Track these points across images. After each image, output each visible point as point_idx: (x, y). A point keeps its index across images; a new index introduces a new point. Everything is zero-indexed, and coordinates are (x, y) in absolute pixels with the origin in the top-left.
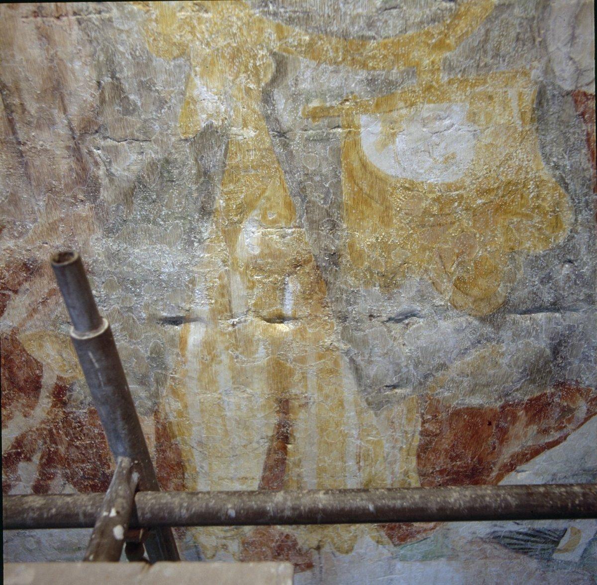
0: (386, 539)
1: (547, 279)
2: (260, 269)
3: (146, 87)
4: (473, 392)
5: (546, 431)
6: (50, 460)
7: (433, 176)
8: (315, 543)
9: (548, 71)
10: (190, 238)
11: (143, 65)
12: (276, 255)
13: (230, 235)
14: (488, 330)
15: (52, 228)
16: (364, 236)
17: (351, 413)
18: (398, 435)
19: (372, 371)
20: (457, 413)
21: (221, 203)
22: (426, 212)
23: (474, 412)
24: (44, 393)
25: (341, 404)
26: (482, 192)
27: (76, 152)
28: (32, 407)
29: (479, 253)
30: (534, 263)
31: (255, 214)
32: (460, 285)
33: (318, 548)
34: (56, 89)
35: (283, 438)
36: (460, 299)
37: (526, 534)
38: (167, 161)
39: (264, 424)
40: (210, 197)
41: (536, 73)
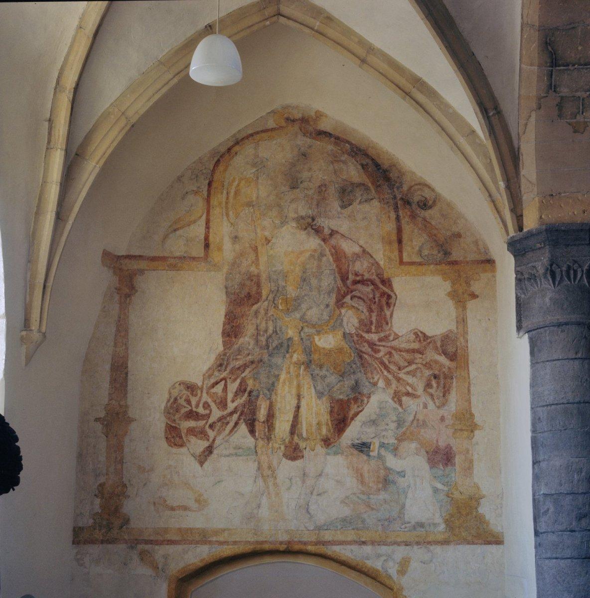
0: (323, 445)
1: (351, 367)
2: (296, 364)
3: (281, 331)
4: (340, 394)
5: (358, 407)
6: (241, 414)
7: (327, 346)
8: (304, 447)
9: (345, 330)
10: (284, 357)
11: (281, 328)
12: (299, 361)
13: (291, 357)
14: (341, 378)
15: (259, 354)
16: (315, 357)
17: (314, 400)
18: (324, 407)
19: (318, 388)
20: (338, 401)
21: (290, 350)
22: (327, 353)
23: (341, 400)
24: (247, 393)
25: (312, 397)
26: (337, 349)
27: (267, 341)
28: (242, 396)
29: (337, 361)
30: (348, 364)
31: (296, 353)
32: (334, 368)
33: (305, 448)
34: (266, 331)
35: (298, 407)
36: (335, 371)
37: (362, 444)
38: (282, 343)
39: (294, 402)
40: (289, 349)
41: (343, 330)
